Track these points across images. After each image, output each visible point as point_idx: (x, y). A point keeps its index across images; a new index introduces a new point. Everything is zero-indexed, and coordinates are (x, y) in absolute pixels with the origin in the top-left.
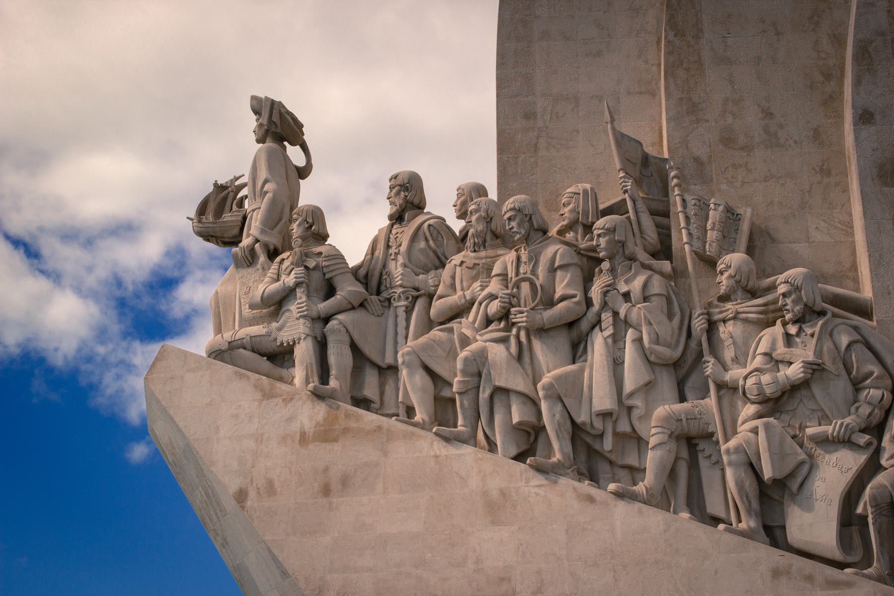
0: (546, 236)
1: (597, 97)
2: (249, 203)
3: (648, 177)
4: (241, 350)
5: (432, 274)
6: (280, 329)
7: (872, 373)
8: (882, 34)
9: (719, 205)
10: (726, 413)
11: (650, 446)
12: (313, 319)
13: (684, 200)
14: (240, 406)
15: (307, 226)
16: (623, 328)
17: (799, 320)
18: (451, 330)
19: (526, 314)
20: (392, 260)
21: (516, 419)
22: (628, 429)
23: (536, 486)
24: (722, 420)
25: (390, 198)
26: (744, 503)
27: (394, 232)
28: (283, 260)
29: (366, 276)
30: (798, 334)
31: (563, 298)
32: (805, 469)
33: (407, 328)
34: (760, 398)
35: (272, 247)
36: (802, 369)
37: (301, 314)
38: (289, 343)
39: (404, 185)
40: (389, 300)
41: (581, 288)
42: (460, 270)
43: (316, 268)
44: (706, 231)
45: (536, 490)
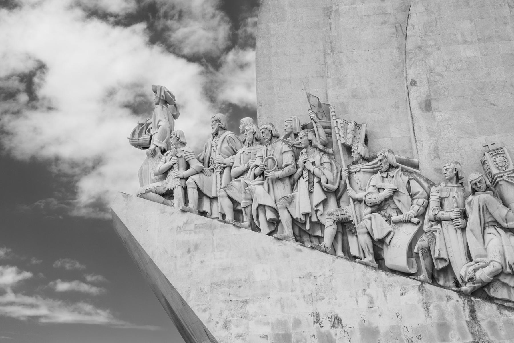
0: (278, 139)
2: (153, 130)
3: (322, 112)
4: (151, 193)
5: (231, 157)
6: (167, 183)
7: (419, 192)
10: (357, 212)
11: (326, 227)
12: (181, 179)
13: (337, 122)
16: (312, 178)
18: (240, 181)
19: (271, 173)
20: (214, 152)
22: (316, 220)
24: (356, 215)
25: (212, 126)
27: (214, 140)
28: (168, 154)
29: (203, 159)
30: (387, 177)
31: (286, 166)
32: (392, 234)
33: (221, 181)
34: (372, 205)
35: (163, 149)
36: (389, 192)
37: (175, 177)
38: (171, 189)
39: (218, 120)
40: (213, 169)
41: (294, 161)
43: (181, 157)
44: (347, 134)
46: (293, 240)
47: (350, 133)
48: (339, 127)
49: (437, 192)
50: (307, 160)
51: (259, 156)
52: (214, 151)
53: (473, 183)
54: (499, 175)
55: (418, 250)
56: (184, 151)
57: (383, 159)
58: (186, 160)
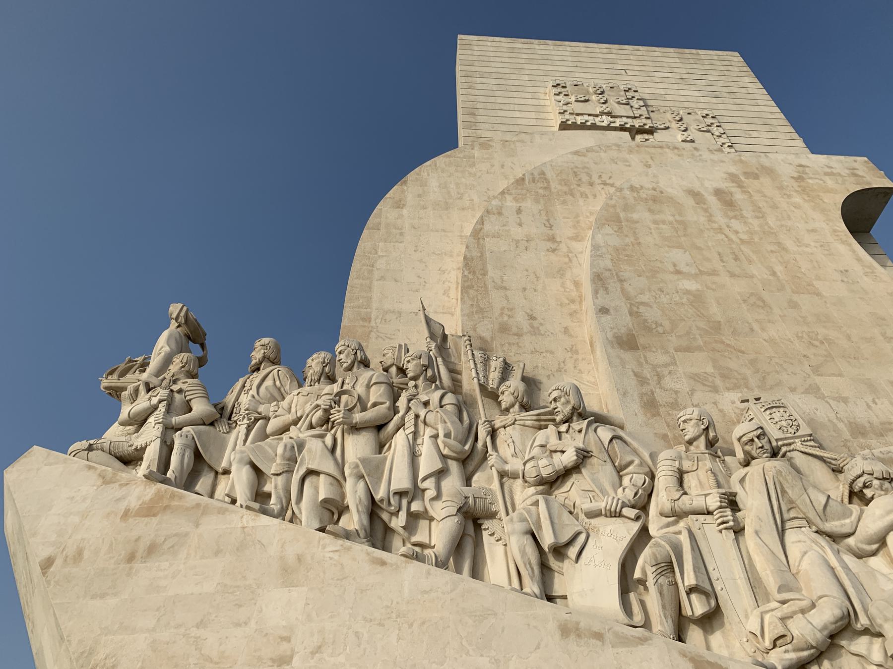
1: (414, 313)
6: (137, 437)
8: (610, 270)
13: (473, 354)
14: (79, 490)
17: (567, 420)
21: (322, 497)
22: (421, 509)
23: (332, 552)
27: (251, 377)
30: (567, 432)
31: (375, 405)
32: (582, 537)
33: (245, 441)
40: (236, 422)
43: (180, 391)
45: (331, 555)
46: (367, 543)
47: (497, 370)
48: (478, 361)
50: (416, 397)
53: (744, 439)
54: (785, 442)
55: (644, 572)
57: (560, 398)
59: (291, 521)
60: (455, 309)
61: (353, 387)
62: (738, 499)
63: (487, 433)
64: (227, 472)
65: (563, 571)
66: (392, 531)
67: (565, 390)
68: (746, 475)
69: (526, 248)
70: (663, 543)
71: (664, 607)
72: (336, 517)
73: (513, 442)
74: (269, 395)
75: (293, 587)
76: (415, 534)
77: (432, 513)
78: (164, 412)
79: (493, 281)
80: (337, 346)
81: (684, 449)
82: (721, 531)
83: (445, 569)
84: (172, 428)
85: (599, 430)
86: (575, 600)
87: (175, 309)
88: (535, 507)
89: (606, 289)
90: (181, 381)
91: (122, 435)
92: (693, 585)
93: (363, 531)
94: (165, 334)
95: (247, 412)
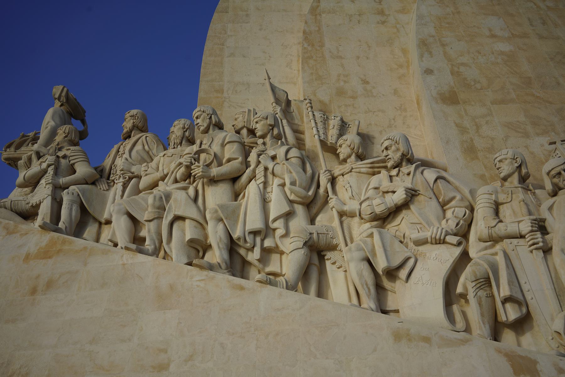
1: (261, 84)
8: (433, 36)
9: (337, 117)
13: (314, 115)
15: (64, 135)
17: (398, 165)
21: (188, 237)
22: (273, 245)
23: (198, 281)
26: (364, 289)
27: (124, 144)
30: (397, 175)
31: (229, 160)
32: (411, 262)
33: (122, 196)
40: (113, 181)
42: (163, 160)
43: (65, 157)
45: (198, 283)
46: (228, 274)
47: (335, 128)
49: (487, 192)
50: (265, 153)
51: (187, 152)
52: (120, 156)
53: (553, 173)
56: (71, 150)
57: (391, 147)
58: (71, 162)
59: (164, 258)
60: (297, 79)
61: (210, 146)
62: (547, 224)
63: (327, 180)
64: (108, 222)
65: (395, 290)
66: (250, 264)
67: (395, 139)
68: (554, 203)
69: (359, 22)
70: (482, 262)
71: (482, 315)
72: (201, 254)
73: (351, 187)
74: (140, 158)
75: (167, 309)
76: (269, 265)
77: (282, 248)
78: (53, 174)
79: (330, 52)
80: (194, 112)
81: (500, 184)
82: (531, 252)
83: (296, 291)
84: (61, 187)
85: (425, 172)
86: (406, 312)
87: (57, 90)
88: (370, 238)
89: (430, 53)
90: (65, 148)
91: (21, 196)
92: (508, 295)
93: (224, 264)
94: (50, 112)
95: (122, 172)
